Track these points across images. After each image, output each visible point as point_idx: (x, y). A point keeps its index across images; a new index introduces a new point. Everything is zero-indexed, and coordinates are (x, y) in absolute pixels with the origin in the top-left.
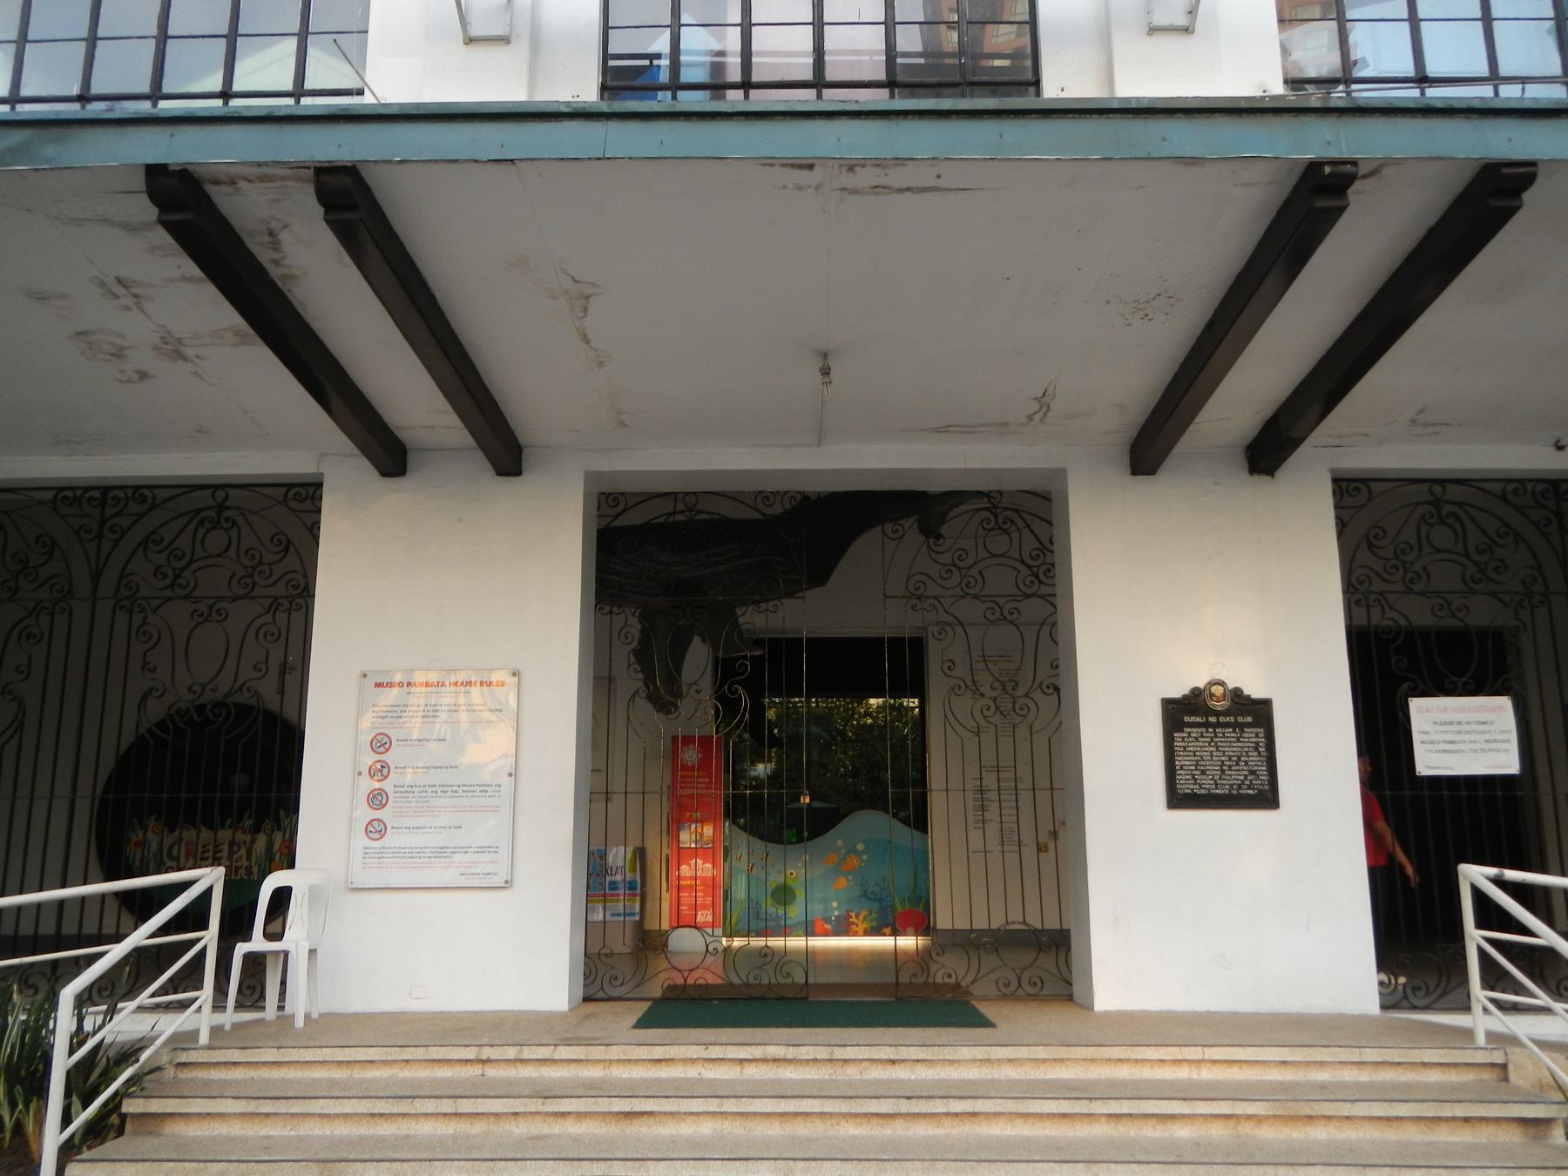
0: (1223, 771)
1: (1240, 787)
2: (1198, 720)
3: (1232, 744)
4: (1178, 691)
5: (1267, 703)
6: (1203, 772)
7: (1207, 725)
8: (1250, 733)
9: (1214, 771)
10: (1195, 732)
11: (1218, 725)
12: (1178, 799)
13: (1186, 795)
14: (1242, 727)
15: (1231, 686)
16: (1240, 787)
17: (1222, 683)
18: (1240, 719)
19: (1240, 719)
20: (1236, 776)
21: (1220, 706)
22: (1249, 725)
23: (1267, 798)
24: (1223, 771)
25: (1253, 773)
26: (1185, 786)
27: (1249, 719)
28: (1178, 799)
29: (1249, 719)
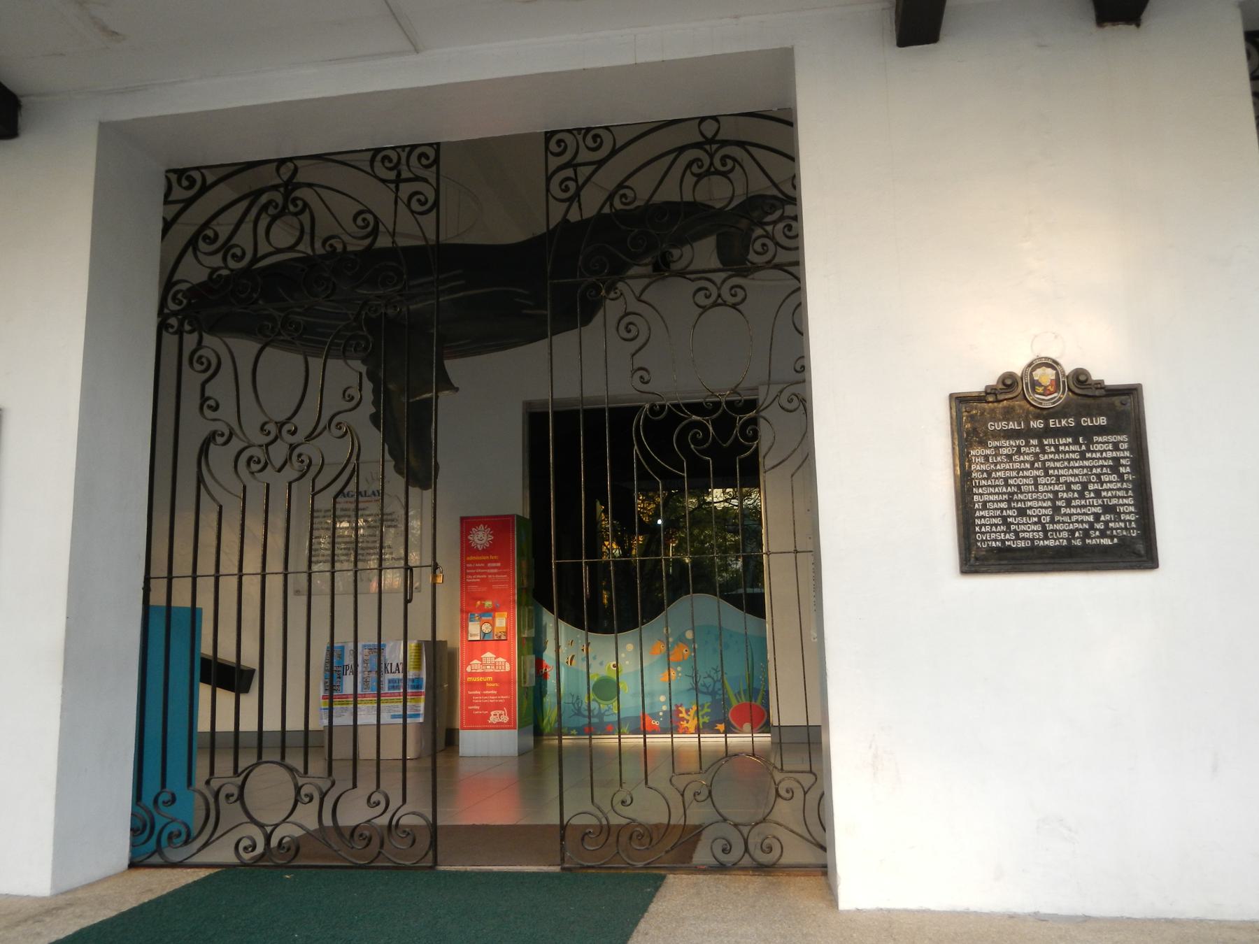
0: (1056, 509)
1: (1086, 534)
2: (1012, 425)
3: (1068, 463)
4: (975, 384)
5: (1132, 393)
6: (1022, 512)
7: (1027, 434)
8: (1102, 443)
9: (1040, 507)
10: (1007, 446)
11: (1048, 432)
12: (978, 558)
13: (991, 549)
14: (1089, 433)
15: (1068, 368)
16: (1086, 534)
17: (1052, 364)
18: (1086, 422)
19: (1086, 422)
20: (1079, 516)
21: (1047, 402)
22: (1101, 430)
23: (1136, 550)
24: (1056, 509)
25: (1108, 509)
26: (990, 536)
27: (1102, 421)
28: (978, 558)
29: (1102, 421)
